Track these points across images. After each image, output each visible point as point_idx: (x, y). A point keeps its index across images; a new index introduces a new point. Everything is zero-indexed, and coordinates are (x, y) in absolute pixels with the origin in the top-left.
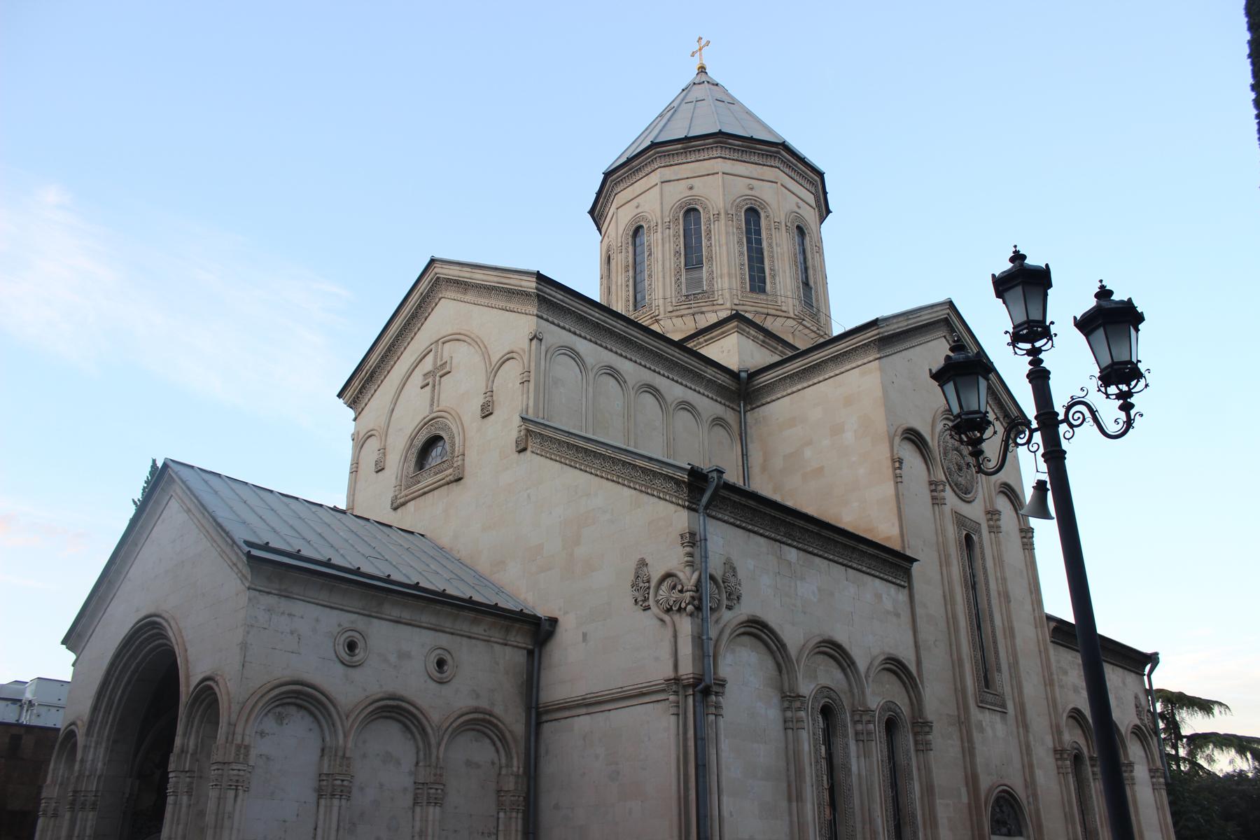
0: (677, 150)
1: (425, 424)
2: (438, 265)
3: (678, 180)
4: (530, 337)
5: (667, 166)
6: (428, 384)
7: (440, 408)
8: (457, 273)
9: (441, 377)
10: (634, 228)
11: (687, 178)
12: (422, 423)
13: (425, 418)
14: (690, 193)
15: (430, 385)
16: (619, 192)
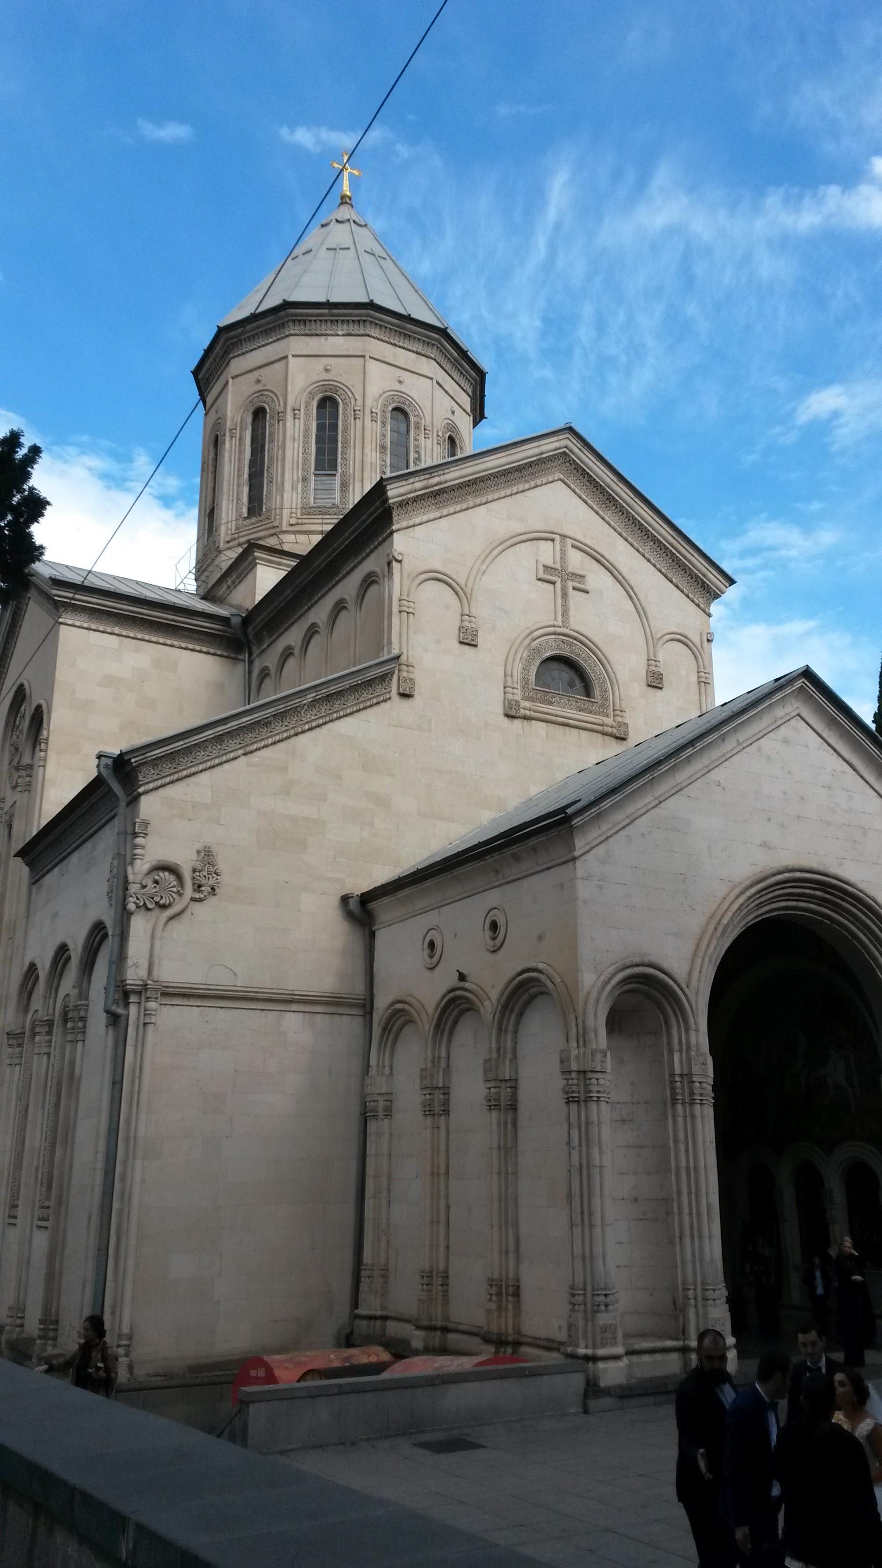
0: (451, 355)
1: (554, 634)
2: (570, 437)
3: (446, 392)
4: (709, 638)
5: (440, 365)
6: (554, 583)
7: (577, 629)
8: (608, 480)
9: (574, 589)
10: (393, 405)
11: (452, 398)
12: (552, 629)
13: (554, 626)
14: (450, 416)
15: (559, 585)
16: (374, 338)
